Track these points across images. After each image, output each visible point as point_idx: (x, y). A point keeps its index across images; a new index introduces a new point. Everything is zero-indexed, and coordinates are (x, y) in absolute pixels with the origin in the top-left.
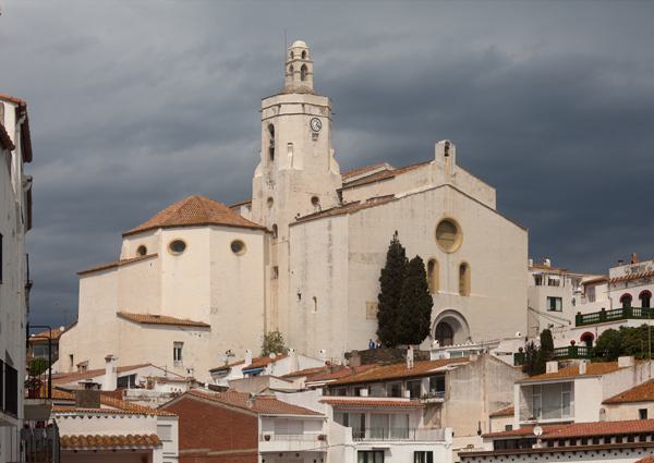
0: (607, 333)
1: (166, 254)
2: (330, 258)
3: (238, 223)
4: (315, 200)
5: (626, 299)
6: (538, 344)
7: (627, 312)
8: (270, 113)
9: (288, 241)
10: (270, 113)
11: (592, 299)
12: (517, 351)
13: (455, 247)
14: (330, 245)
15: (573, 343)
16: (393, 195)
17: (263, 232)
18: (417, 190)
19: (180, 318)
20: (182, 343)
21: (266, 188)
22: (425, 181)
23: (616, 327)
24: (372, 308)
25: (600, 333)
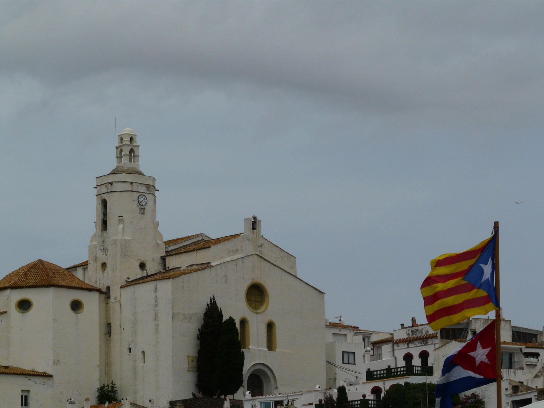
0: (392, 387)
1: (14, 312)
2: (156, 317)
3: (76, 285)
4: (142, 266)
5: (408, 357)
6: (335, 397)
7: (409, 370)
9: (120, 301)
11: (380, 357)
12: (318, 403)
13: (263, 308)
14: (156, 306)
15: (364, 396)
16: (210, 263)
17: (98, 293)
18: (229, 259)
19: (26, 369)
20: (28, 391)
21: (100, 254)
22: (236, 251)
23: (402, 381)
24: (193, 361)
25: (387, 388)
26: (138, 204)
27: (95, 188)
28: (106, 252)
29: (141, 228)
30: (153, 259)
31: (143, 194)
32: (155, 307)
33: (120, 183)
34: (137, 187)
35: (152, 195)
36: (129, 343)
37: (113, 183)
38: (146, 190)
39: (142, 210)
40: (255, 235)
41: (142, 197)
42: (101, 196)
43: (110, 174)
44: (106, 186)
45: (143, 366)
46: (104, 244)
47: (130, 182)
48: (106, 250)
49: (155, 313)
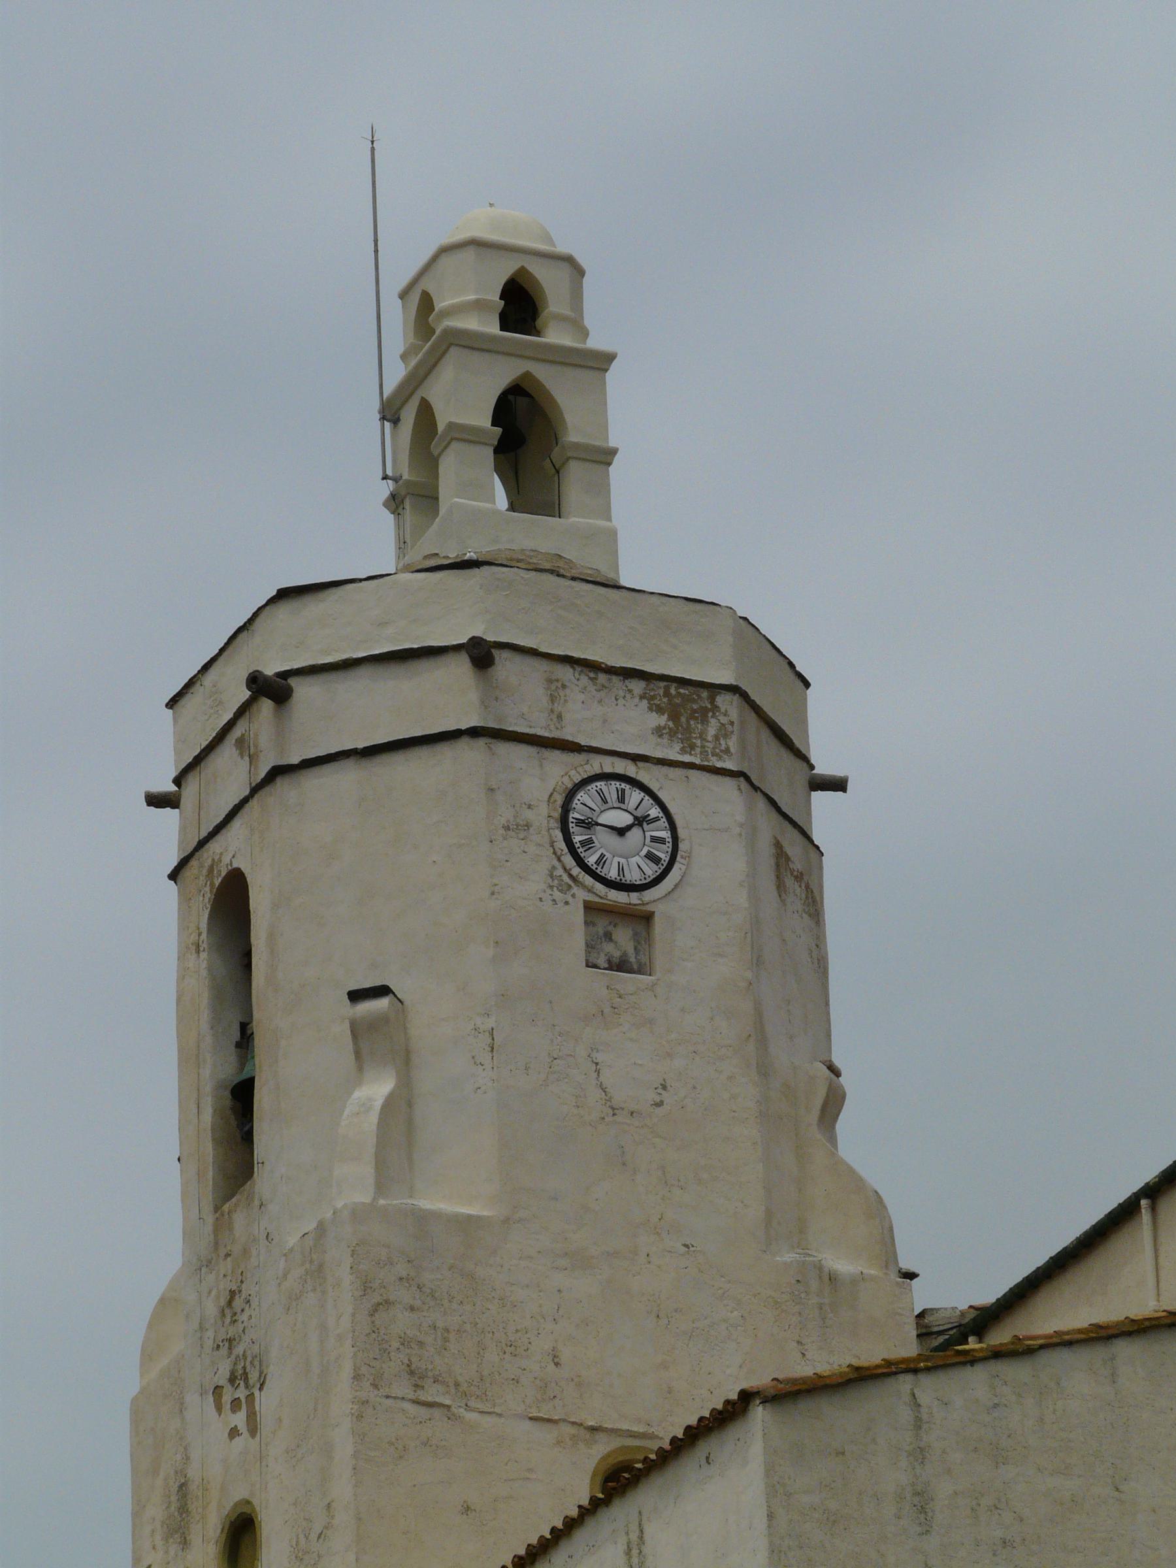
26: (569, 860)
27: (156, 801)
28: (250, 1398)
29: (614, 1110)
31: (630, 769)
33: (364, 671)
34: (553, 699)
35: (729, 782)
37: (292, 682)
38: (658, 731)
39: (624, 938)
41: (612, 797)
42: (209, 862)
43: (272, 601)
44: (241, 743)
47: (457, 648)
48: (253, 1376)
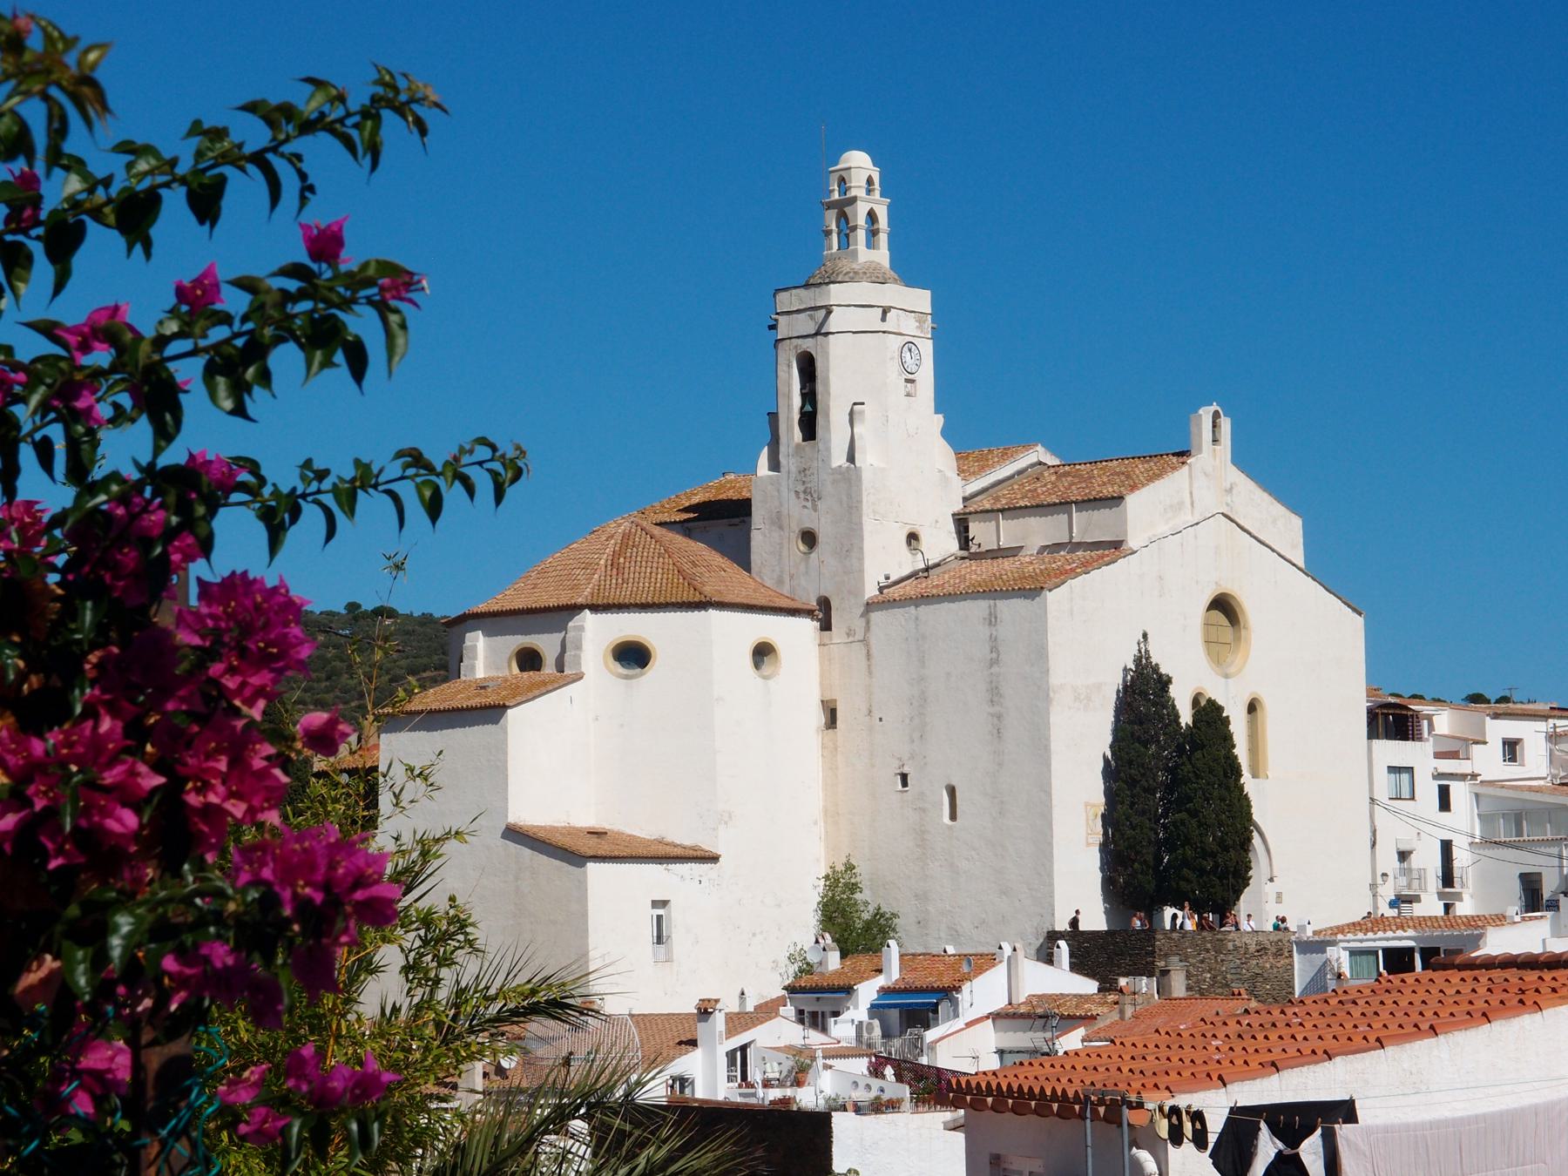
2: (995, 693)
8: (804, 324)
9: (865, 641)
10: (804, 324)
22: (1180, 506)
30: (937, 522)
31: (911, 339)
32: (991, 666)
36: (900, 759)
38: (917, 327)
40: (1218, 460)
45: (950, 828)
46: (805, 476)
49: (991, 682)
